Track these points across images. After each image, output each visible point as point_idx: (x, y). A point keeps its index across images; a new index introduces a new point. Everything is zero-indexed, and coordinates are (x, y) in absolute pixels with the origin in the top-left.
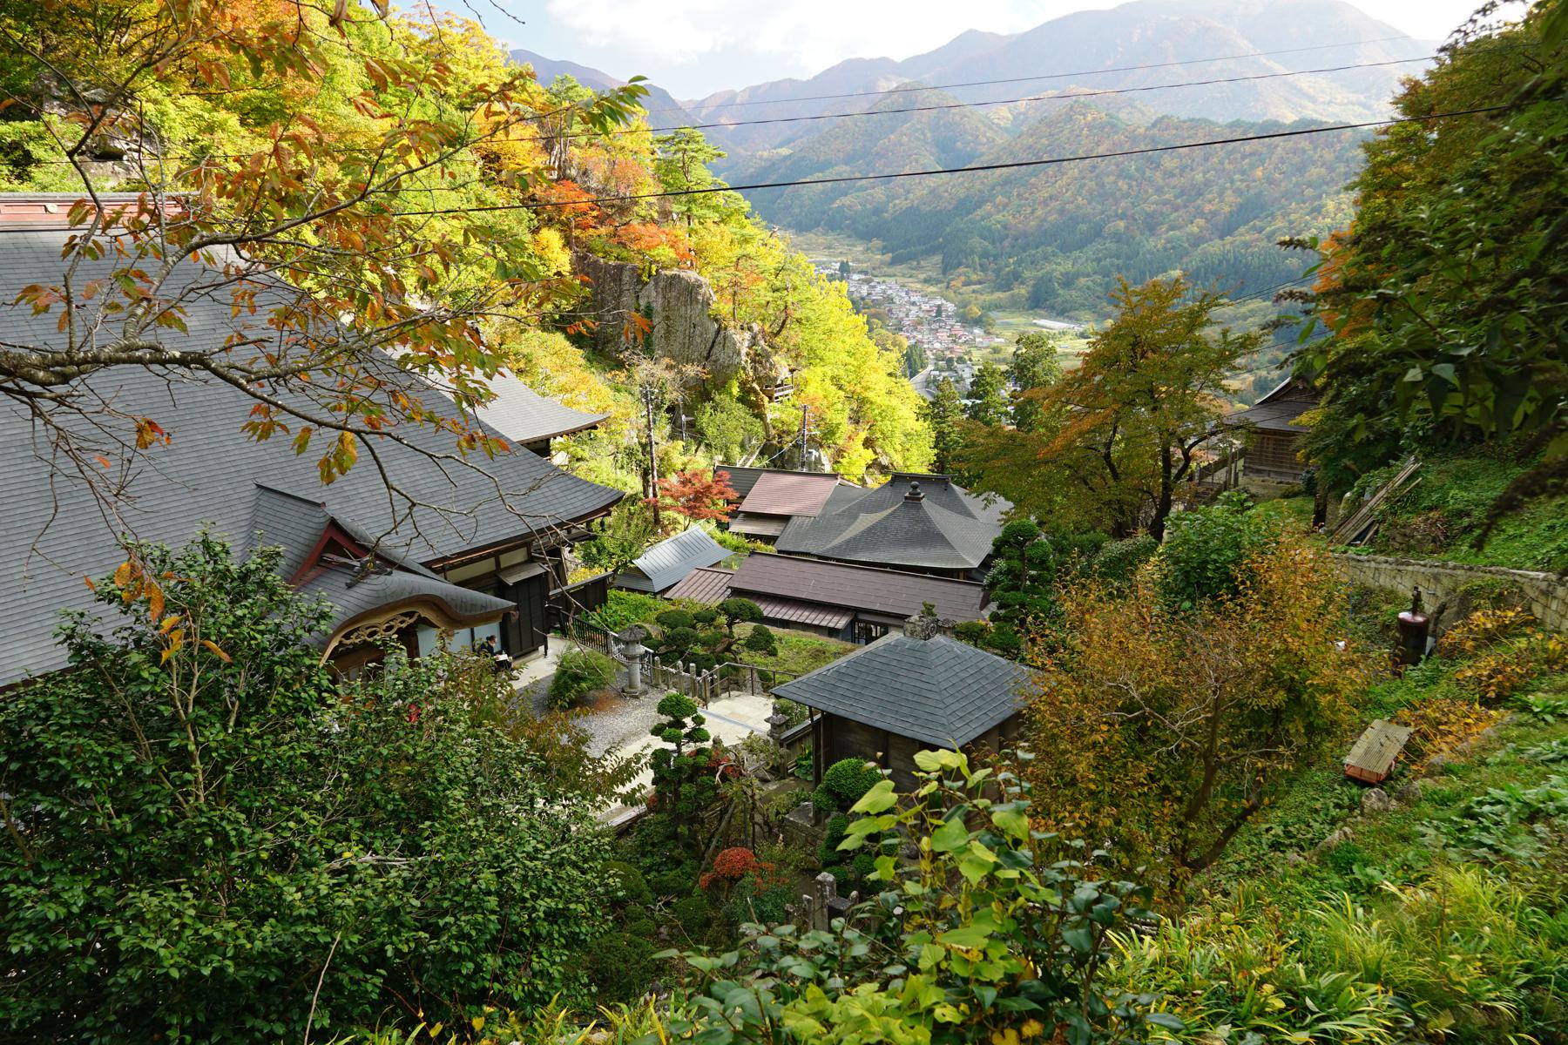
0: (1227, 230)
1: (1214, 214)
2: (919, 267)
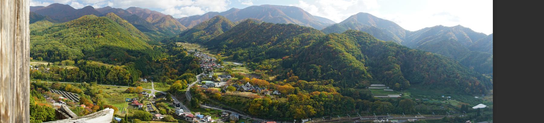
0: (274, 44)
1: (273, 41)
2: (213, 51)
